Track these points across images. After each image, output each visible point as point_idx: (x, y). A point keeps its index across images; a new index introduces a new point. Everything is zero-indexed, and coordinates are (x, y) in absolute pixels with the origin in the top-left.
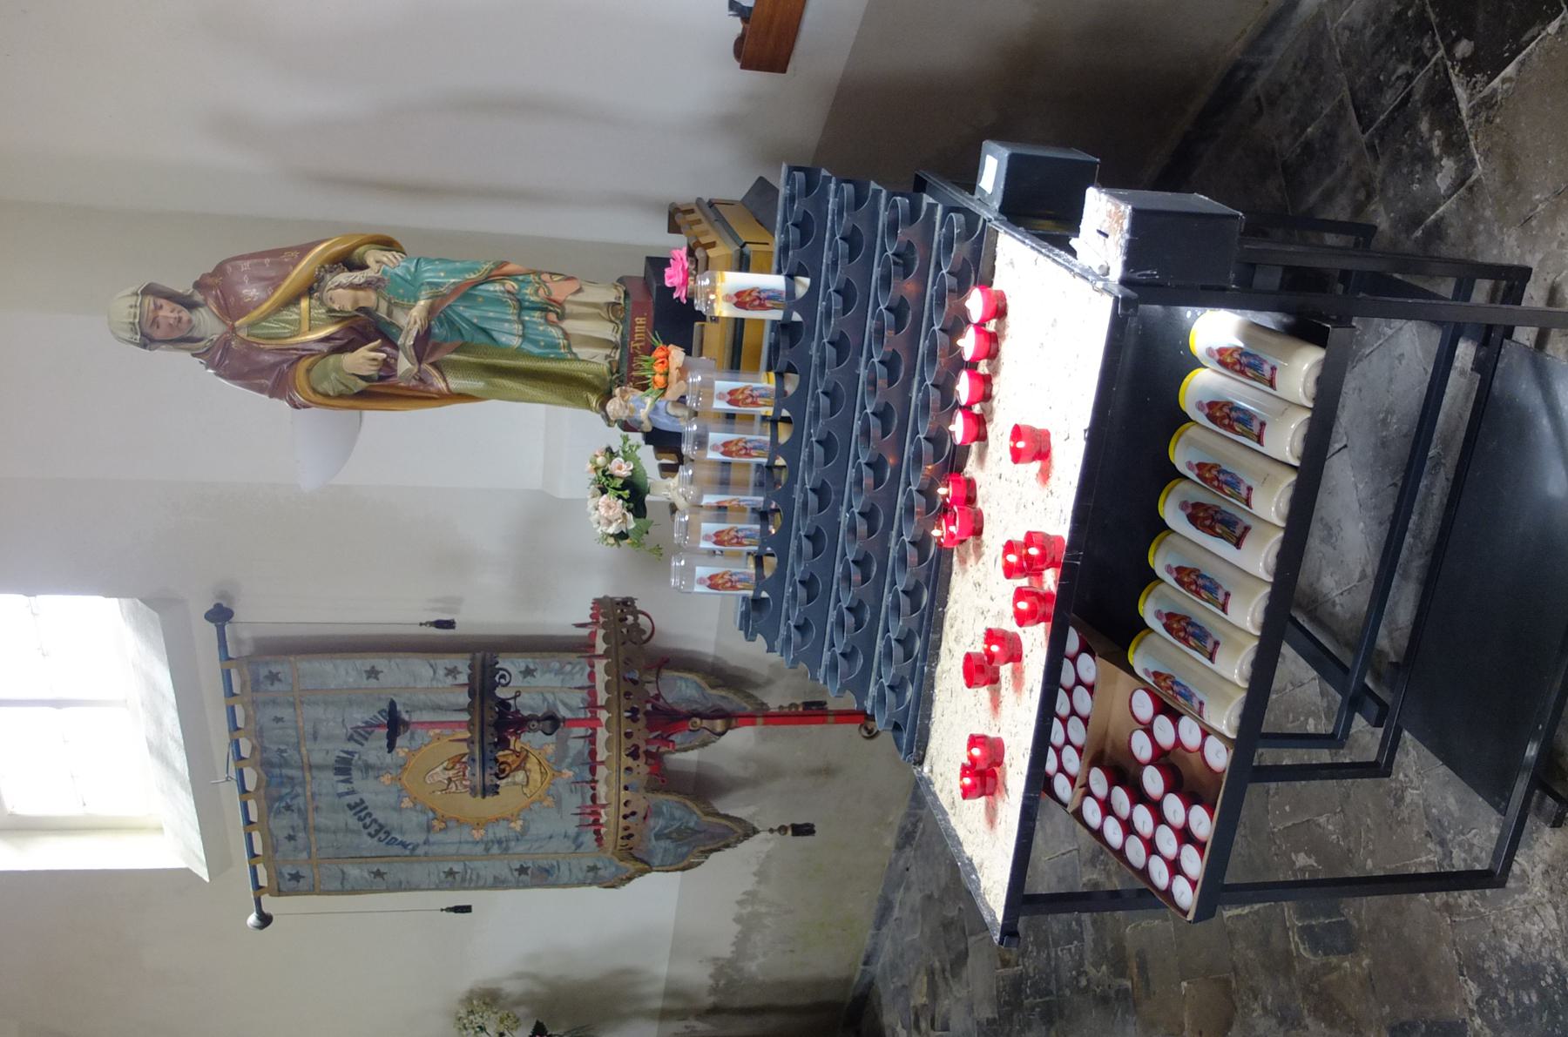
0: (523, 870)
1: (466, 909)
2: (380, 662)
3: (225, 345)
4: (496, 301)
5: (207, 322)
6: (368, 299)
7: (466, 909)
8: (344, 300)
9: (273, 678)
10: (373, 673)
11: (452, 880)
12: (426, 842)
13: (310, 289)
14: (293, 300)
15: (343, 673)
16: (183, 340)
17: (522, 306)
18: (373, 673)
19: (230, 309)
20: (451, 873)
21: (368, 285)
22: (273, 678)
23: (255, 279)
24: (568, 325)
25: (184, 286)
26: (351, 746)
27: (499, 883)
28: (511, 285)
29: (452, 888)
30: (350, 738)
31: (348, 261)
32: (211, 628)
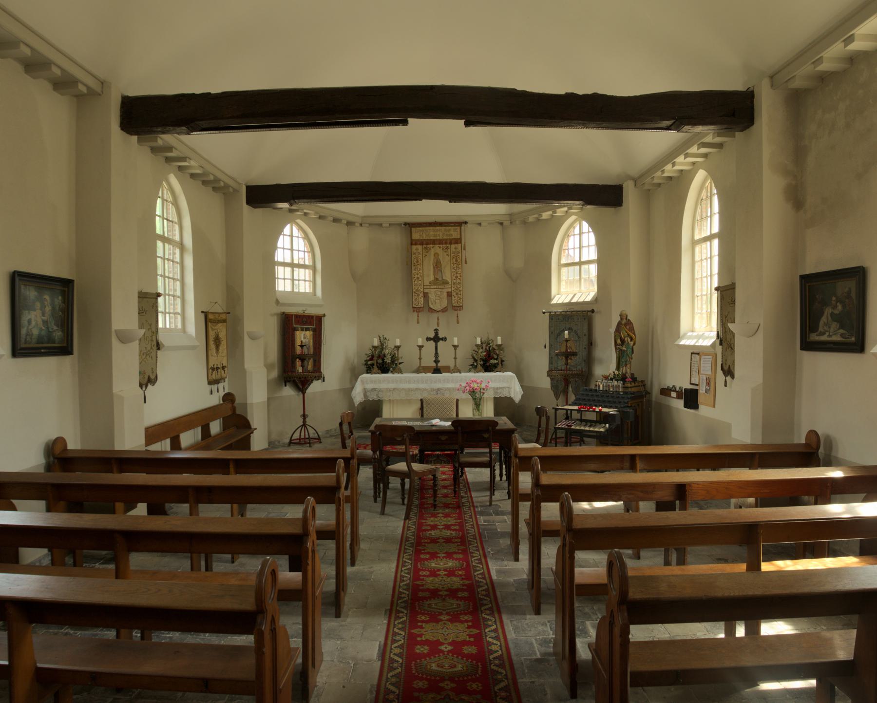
0: (552, 358)
1: (545, 348)
2: (587, 336)
3: (621, 324)
4: (626, 358)
5: (624, 322)
6: (627, 342)
7: (545, 348)
8: (626, 339)
9: (585, 319)
10: (585, 335)
11: (551, 346)
12: (557, 342)
13: (629, 335)
14: (627, 333)
15: (585, 331)
16: (622, 319)
17: (626, 362)
18: (585, 335)
19: (626, 325)
20: (552, 345)
21: (628, 342)
22: (585, 319)
23: (629, 328)
24: (624, 367)
25: (628, 318)
26: (574, 330)
27: (550, 354)
28: (628, 360)
29: (549, 346)
30: (575, 330)
31: (632, 339)
32: (591, 310)
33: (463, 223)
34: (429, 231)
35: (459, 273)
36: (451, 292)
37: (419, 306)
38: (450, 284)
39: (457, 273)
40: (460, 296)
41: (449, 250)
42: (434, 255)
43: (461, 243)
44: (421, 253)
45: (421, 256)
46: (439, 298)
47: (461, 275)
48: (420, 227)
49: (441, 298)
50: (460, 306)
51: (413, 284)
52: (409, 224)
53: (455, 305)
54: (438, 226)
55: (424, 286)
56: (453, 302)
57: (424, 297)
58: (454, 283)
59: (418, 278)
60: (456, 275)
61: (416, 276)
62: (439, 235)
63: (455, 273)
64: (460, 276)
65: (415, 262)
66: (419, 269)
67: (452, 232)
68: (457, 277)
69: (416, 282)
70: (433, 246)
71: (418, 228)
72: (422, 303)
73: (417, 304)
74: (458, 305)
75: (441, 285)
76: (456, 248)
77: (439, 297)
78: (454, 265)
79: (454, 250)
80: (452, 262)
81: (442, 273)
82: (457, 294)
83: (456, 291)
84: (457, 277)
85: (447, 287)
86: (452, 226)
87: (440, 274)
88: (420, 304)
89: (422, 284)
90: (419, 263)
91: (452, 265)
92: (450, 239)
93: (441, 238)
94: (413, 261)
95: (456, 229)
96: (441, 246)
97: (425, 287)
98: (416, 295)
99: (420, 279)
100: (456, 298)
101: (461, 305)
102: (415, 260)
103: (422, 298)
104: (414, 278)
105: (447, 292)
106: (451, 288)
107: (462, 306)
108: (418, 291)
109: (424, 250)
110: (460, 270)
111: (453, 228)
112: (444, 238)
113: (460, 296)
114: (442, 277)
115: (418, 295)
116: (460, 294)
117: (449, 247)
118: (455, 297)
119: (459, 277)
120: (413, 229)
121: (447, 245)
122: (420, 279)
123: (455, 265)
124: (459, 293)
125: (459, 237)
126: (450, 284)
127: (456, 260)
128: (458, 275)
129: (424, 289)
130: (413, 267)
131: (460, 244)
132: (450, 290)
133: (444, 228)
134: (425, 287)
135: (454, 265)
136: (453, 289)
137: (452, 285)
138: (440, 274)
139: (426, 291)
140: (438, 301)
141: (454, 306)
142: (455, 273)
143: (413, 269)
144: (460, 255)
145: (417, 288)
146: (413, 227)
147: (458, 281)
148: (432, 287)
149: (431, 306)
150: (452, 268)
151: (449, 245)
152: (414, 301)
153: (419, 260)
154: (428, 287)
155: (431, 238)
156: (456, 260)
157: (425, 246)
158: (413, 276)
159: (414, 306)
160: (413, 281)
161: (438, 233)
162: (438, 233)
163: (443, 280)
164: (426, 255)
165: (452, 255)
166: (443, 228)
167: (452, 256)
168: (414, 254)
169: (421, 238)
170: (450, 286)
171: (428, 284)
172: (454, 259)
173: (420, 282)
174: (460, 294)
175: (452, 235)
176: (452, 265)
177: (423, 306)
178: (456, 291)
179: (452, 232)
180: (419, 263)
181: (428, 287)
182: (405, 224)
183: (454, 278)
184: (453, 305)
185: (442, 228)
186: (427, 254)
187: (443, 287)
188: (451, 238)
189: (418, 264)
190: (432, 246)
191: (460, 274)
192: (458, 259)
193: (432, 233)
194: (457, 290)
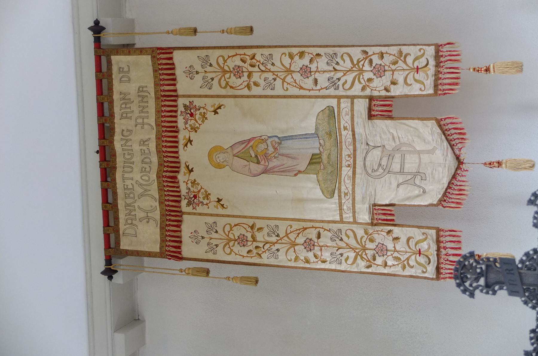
33: (97, 41)
34: (128, 183)
35: (287, 61)
36: (371, 99)
37: (434, 247)
38: (333, 102)
39: (289, 71)
40: (387, 59)
41: (198, 102)
42: (219, 166)
43: (169, 51)
44: (211, 220)
45: (222, 222)
46: (398, 157)
47: (295, 51)
48: (117, 219)
49: (397, 149)
50: (437, 56)
51: (333, 267)
52: (108, 261)
53: (429, 82)
54: (112, 142)
55: (342, 221)
56: (415, 90)
57: (391, 222)
58: (334, 83)
59: (309, 245)
60: (297, 76)
61: (303, 254)
62: (143, 142)
63: (289, 79)
64: (302, 55)
65: (244, 251)
66: (274, 239)
67: (132, 88)
68: (306, 71)
69: (326, 255)
70: (183, 169)
71: (122, 227)
72: (417, 234)
73: (422, 260)
74: (431, 69)
75: (338, 144)
76: (191, 73)
77: (391, 157)
78: (256, 84)
79: (198, 78)
80: (246, 92)
81: (291, 138)
82: (379, 71)
83: (367, 75)
84: (306, 71)
85: (345, 121)
86: (110, 89)
87: (290, 147)
88: (424, 246)
89: (335, 227)
90: (249, 235)
91: (255, 91)
92: (157, 98)
93: (153, 136)
94: (239, 259)
95: (120, 70)
96: (182, 136)
97: (348, 216)
98: (379, 260)
99: (314, 237)
100: (400, 77)
101: (431, 51)
102: (237, 248)
103: (396, 230)
104: (307, 261)
105: (371, 116)
106: (353, 98)
107: (438, 48)
108: (364, 249)
109: (200, 209)
110: (277, 53)
111: (115, 83)
112: (152, 121)
113: (387, 59)
114: (306, 136)
115: (382, 250)
116: (382, 56)
117: (186, 101)
118: (394, 83)
119: (306, 61)
120: (125, 245)
121: (181, 108)
122: (314, 237)
123: (256, 77)
124: (376, 60)
125: (147, 59)
126: (333, 102)
127: (238, 72)
128: (299, 63)
129: (355, 222)
130: (265, 259)
131: (177, 56)
132: (361, 106)
133: (116, 120)
134: (348, 216)
135: (256, 84)
136: (356, 90)
137: (341, 92)
138: (290, 147)
139: (364, 217)
140: (411, 165)
141: (436, 86)
142: (289, 79)
143: (272, 261)
144: (214, 55)
145: (352, 255)
146: (118, 243)
147: (322, 63)
148: (346, 185)
149: (433, 197)
150: (269, 92)
151: (181, 102)
152: (408, 272)
153: (237, 232)
154: (347, 204)
155: (154, 176)
156: (238, 72)
157: (184, 203)
158: (301, 264)
159: (431, 270)
160: (323, 266)
161: (136, 147)
162: (136, 147)
163: (316, 135)
164: (219, 200)
165: (216, 90)
166: (120, 125)
167: (223, 92)
168: (213, 248)
169: (157, 215)
170: (345, 104)
171: (332, 204)
172: (234, 81)
173: (325, 240)
174: (382, 56)
175: (141, 89)
176: (255, 91)
177: (433, 232)
178: (367, 76)
179: (132, 88)
180: (249, 235)
181: (347, 204)
182: (109, 273)
183: (308, 83)
184: (431, 91)
185: (117, 130)
186: (213, 198)
187: (346, 135)
188: (153, 95)
189: (254, 240)
190: (181, 177)
191: (291, 57)
192: (232, 64)
193: (137, 176)
194: (361, 71)
